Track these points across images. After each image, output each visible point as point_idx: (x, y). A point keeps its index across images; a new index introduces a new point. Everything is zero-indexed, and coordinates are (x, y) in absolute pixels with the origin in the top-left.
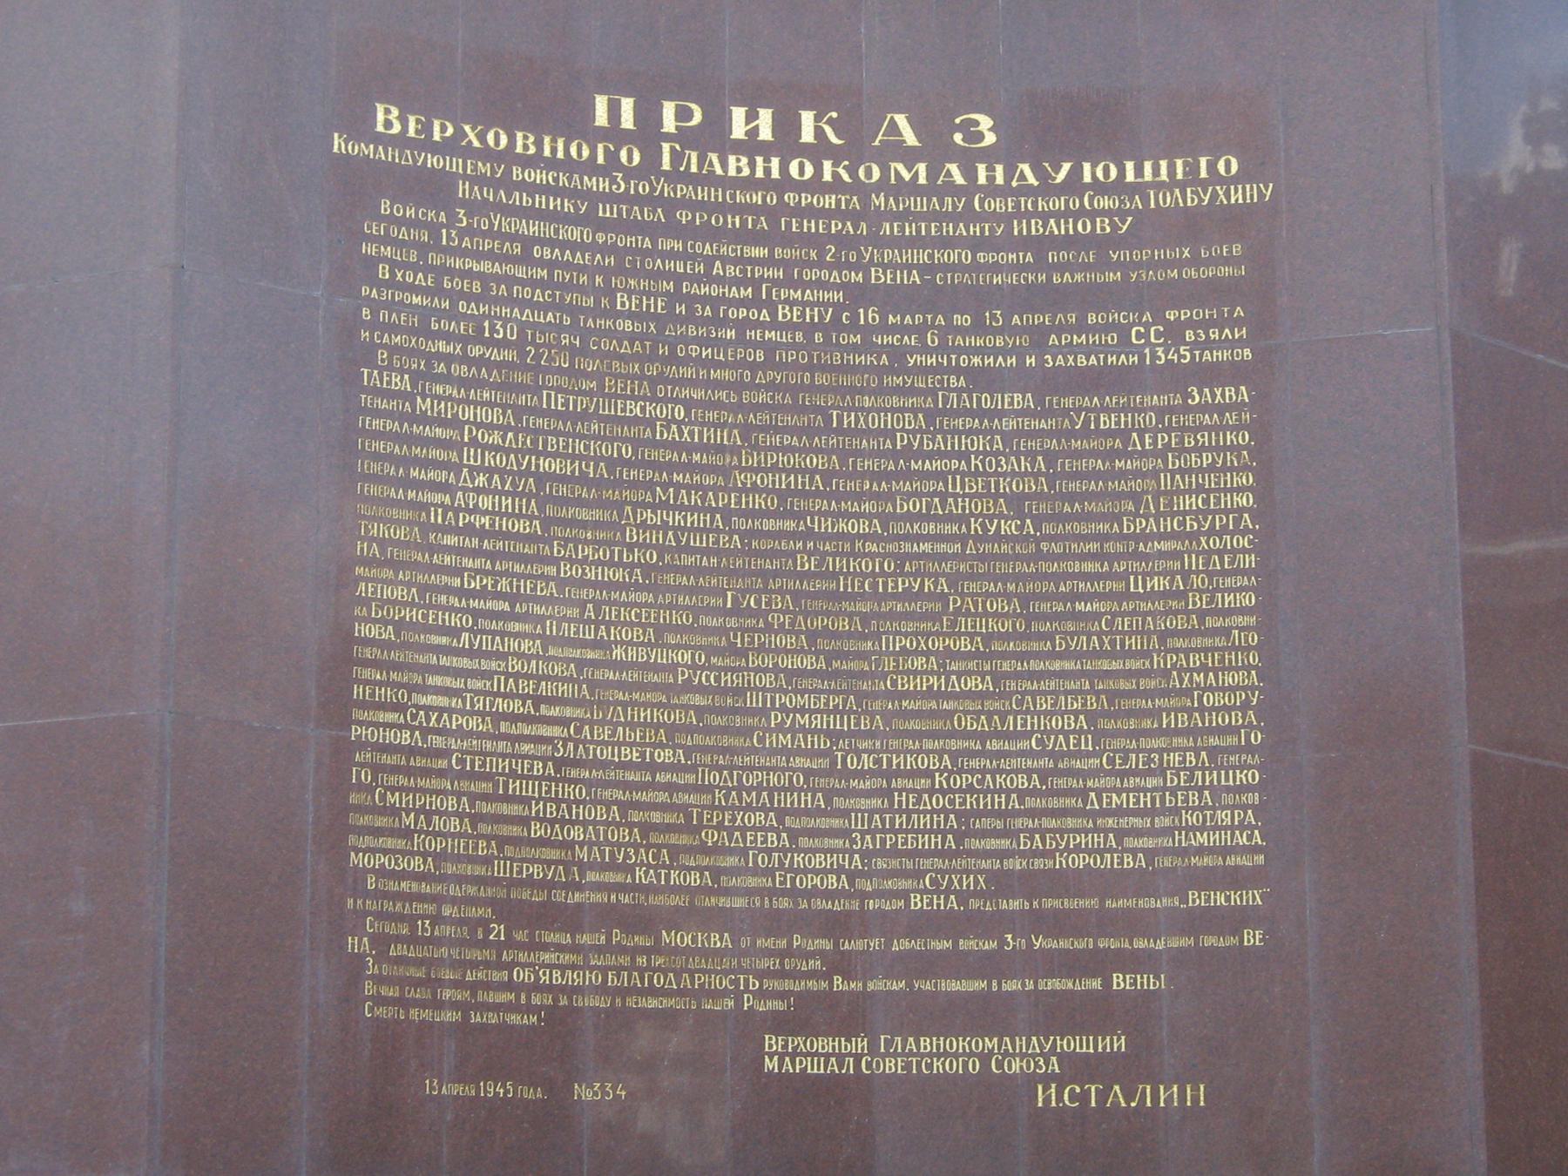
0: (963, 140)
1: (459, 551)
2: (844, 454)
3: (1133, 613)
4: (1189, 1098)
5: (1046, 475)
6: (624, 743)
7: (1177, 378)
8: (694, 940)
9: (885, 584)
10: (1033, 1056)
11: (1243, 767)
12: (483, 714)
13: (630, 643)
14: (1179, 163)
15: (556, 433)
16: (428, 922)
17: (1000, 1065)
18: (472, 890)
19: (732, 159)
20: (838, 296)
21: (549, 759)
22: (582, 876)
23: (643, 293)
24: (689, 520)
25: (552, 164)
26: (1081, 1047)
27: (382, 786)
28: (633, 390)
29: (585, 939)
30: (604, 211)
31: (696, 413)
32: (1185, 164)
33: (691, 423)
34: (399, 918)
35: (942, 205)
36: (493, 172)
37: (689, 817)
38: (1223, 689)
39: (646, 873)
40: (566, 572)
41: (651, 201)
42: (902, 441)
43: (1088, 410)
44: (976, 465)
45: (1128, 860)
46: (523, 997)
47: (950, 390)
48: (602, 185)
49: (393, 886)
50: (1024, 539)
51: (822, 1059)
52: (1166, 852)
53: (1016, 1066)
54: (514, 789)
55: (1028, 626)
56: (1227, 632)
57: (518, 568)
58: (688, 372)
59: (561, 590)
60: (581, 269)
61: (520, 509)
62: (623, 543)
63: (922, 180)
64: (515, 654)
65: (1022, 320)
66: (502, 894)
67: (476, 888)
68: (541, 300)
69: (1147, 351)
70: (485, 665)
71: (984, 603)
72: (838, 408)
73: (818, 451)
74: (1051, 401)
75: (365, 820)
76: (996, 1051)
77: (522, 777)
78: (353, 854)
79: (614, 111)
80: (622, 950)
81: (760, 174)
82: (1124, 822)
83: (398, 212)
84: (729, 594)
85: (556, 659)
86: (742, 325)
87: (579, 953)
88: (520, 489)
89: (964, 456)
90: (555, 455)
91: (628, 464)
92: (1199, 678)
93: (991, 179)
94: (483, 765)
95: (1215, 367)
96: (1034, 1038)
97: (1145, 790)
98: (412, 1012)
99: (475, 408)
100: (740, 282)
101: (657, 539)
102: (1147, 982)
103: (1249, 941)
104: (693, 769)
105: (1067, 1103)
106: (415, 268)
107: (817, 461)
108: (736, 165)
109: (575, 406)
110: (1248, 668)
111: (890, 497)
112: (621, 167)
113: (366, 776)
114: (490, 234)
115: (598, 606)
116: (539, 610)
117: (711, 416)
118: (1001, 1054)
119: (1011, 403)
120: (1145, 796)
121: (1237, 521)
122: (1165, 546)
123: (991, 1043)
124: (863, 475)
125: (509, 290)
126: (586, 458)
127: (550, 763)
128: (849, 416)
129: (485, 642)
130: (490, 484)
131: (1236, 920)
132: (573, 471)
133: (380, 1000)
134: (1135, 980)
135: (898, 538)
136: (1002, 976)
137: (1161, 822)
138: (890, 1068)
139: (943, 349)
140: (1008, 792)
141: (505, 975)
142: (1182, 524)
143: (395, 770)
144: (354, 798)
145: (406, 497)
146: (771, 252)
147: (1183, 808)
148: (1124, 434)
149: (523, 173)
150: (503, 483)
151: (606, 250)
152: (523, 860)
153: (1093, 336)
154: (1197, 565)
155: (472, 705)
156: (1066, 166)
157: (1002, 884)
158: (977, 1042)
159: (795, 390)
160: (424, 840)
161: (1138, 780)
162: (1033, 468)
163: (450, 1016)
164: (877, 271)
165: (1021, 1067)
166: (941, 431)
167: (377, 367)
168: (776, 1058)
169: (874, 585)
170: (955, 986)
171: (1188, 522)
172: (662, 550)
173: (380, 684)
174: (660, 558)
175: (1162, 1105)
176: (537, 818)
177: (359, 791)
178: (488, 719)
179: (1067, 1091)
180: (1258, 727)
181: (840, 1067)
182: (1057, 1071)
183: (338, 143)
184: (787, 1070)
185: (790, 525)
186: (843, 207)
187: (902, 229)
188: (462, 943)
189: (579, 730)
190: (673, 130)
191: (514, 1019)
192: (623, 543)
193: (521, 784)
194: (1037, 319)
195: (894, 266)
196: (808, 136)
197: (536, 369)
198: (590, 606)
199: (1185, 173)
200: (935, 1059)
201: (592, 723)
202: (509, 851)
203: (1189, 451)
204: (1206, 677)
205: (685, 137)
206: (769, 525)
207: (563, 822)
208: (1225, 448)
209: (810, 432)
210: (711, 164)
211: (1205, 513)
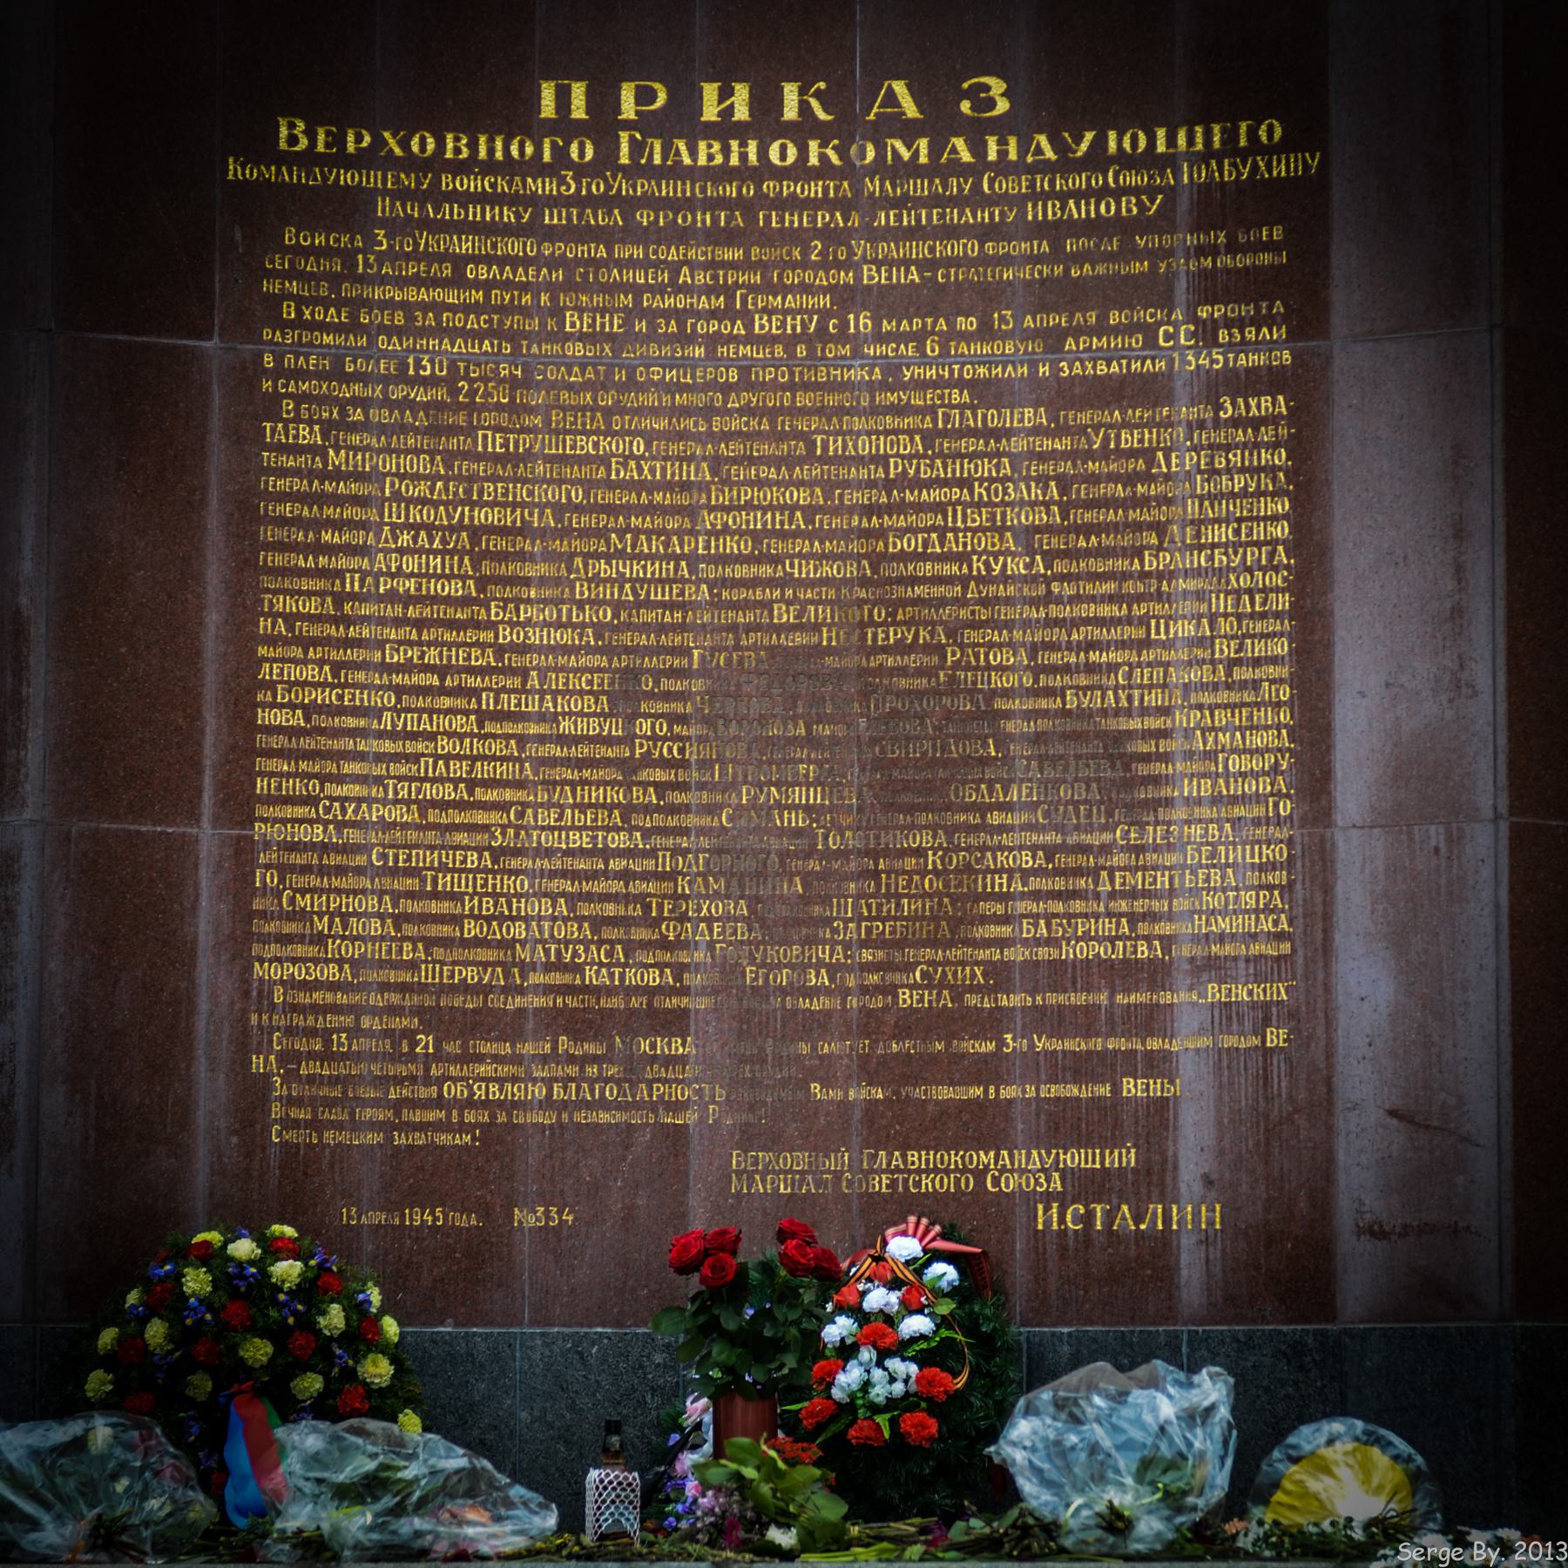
1: (382, 621)
2: (829, 486)
5: (1059, 504)
6: (573, 828)
9: (875, 636)
12: (408, 802)
13: (581, 714)
14: (1216, 128)
15: (495, 479)
17: (996, 1182)
18: (395, 998)
19: (702, 145)
20: (825, 301)
21: (485, 849)
22: (523, 977)
23: (594, 310)
24: (649, 570)
25: (490, 167)
28: (584, 424)
29: (528, 1049)
30: (551, 218)
32: (1223, 132)
33: (653, 458)
34: (311, 1033)
35: (945, 188)
36: (419, 183)
37: (647, 908)
38: (1251, 752)
39: (598, 972)
40: (505, 637)
41: (607, 202)
42: (896, 467)
44: (980, 495)
45: (1143, 951)
46: (455, 1113)
48: (547, 187)
49: (304, 999)
50: (1033, 579)
54: (445, 885)
55: (1036, 681)
56: (1256, 685)
57: (448, 637)
58: (650, 399)
60: (524, 287)
61: (452, 569)
62: (573, 601)
63: (923, 159)
64: (445, 733)
65: (1035, 322)
66: (429, 1002)
67: (399, 996)
69: (1176, 355)
71: (987, 655)
72: (825, 432)
73: (800, 484)
74: (1066, 417)
75: (271, 927)
77: (454, 870)
80: (571, 1059)
81: (734, 160)
82: (1140, 905)
84: (696, 652)
85: (495, 736)
86: (713, 341)
87: (520, 1064)
89: (965, 483)
90: (494, 504)
91: (578, 509)
93: (1003, 154)
94: (409, 859)
96: (1035, 1152)
98: (326, 1135)
100: (709, 291)
102: (1157, 1088)
104: (652, 853)
107: (801, 496)
108: (707, 153)
109: (516, 447)
112: (570, 164)
113: (272, 879)
114: (415, 256)
115: (543, 673)
116: (472, 682)
117: (675, 448)
124: (851, 510)
125: (438, 319)
126: (533, 505)
127: (486, 854)
128: (835, 442)
129: (410, 722)
130: (415, 542)
132: (514, 522)
133: (288, 1124)
134: (1148, 1085)
136: (999, 1080)
140: (1010, 872)
142: (1211, 558)
143: (306, 869)
144: (257, 904)
145: (316, 564)
146: (747, 253)
148: (1148, 454)
150: (431, 541)
151: (553, 263)
152: (454, 963)
155: (396, 793)
156: (1089, 136)
157: (1000, 977)
159: (773, 413)
162: (1044, 495)
163: (373, 1138)
164: (870, 270)
167: (282, 420)
170: (944, 1093)
172: (618, 606)
173: (289, 775)
174: (616, 615)
176: (471, 916)
180: (1288, 796)
182: (1060, 1189)
183: (234, 170)
185: (766, 571)
187: (899, 218)
189: (521, 815)
190: (632, 116)
191: (444, 1139)
192: (573, 601)
194: (1053, 320)
195: (889, 263)
196: (791, 113)
197: (471, 407)
199: (1223, 142)
202: (439, 953)
205: (648, 125)
206: (741, 571)
207: (501, 919)
208: (1259, 469)
209: (789, 461)
210: (678, 153)
211: (1236, 546)
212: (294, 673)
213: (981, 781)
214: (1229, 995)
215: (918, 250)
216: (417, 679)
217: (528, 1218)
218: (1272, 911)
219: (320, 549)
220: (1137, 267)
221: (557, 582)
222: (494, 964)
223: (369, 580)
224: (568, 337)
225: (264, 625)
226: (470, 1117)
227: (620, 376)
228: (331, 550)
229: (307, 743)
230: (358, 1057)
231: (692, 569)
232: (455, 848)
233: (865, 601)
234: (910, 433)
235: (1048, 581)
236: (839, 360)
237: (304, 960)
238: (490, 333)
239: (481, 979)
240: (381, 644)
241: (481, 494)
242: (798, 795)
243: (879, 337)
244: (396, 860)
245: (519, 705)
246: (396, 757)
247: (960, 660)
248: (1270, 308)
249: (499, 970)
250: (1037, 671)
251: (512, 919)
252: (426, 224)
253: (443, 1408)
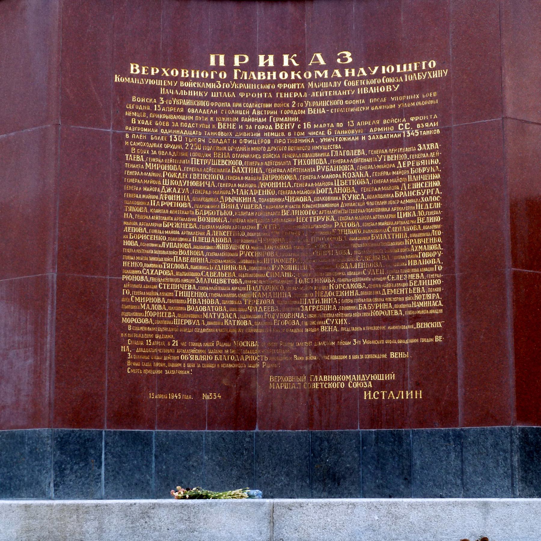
0: (341, 61)
1: (162, 215)
2: (298, 175)
3: (398, 226)
4: (416, 395)
5: (369, 178)
6: (221, 278)
7: (414, 141)
8: (245, 344)
9: (313, 219)
10: (363, 381)
11: (436, 278)
12: (170, 270)
13: (223, 243)
14: (415, 64)
15: (196, 172)
16: (150, 340)
17: (351, 385)
18: (166, 329)
19: (259, 73)
20: (296, 119)
21: (194, 284)
22: (206, 323)
23: (227, 122)
25: (195, 80)
26: (379, 378)
27: (134, 295)
29: (207, 345)
30: (214, 95)
31: (246, 163)
32: (418, 65)
33: (245, 166)
35: (333, 85)
36: (173, 84)
38: (429, 251)
39: (228, 321)
40: (200, 220)
41: (231, 90)
42: (319, 168)
43: (383, 154)
44: (344, 176)
45: (396, 313)
46: (184, 364)
47: (335, 150)
52: (410, 309)
53: (357, 385)
54: (181, 295)
55: (362, 232)
56: (430, 231)
57: (182, 220)
58: (244, 149)
59: (198, 226)
60: (205, 115)
61: (183, 199)
62: (220, 209)
63: (326, 76)
65: (361, 124)
67: (167, 328)
68: (191, 127)
69: (404, 132)
70: (171, 253)
71: (347, 224)
72: (296, 158)
73: (289, 174)
74: (370, 152)
75: (127, 307)
77: (184, 290)
78: (123, 318)
79: (217, 60)
80: (220, 348)
81: (269, 78)
82: (395, 299)
83: (139, 100)
84: (258, 225)
85: (196, 250)
86: (263, 131)
87: (204, 349)
88: (183, 192)
89: (340, 173)
90: (196, 180)
91: (222, 182)
92: (421, 247)
93: (350, 74)
94: (170, 287)
95: (426, 136)
96: (363, 375)
97: (402, 288)
98: (144, 371)
99: (167, 165)
100: (261, 116)
101: (232, 207)
102: (402, 355)
103: (437, 340)
104: (245, 285)
105: (374, 398)
106: (145, 119)
107: (289, 177)
108: (261, 76)
109: (203, 163)
110: (437, 243)
111: (314, 188)
112: (219, 79)
113: (128, 292)
116: (190, 233)
117: (252, 163)
119: (357, 153)
120: (402, 290)
121: (434, 191)
122: (410, 201)
123: (348, 377)
124: (305, 181)
126: (208, 181)
127: (194, 285)
128: (300, 161)
129: (171, 245)
130: (172, 191)
131: (432, 333)
132: (202, 185)
133: (133, 367)
134: (398, 354)
135: (317, 202)
136: (352, 354)
137: (408, 299)
139: (333, 135)
140: (355, 290)
141: (178, 358)
142: (415, 193)
143: (137, 290)
144: (123, 300)
145: (142, 197)
146: (273, 105)
147: (415, 294)
148: (396, 162)
149: (184, 84)
150: (177, 191)
151: (214, 108)
152: (184, 319)
153: (385, 128)
154: (421, 208)
155: (166, 267)
156: (376, 68)
157: (352, 322)
158: (344, 377)
159: (281, 153)
160: (149, 313)
161: (400, 284)
163: (159, 372)
164: (310, 110)
165: (359, 385)
166: (332, 164)
167: (131, 154)
169: (309, 220)
170: (335, 358)
171: (417, 192)
172: (234, 211)
173: (133, 261)
174: (233, 213)
175: (407, 398)
176: (189, 304)
177: (125, 297)
178: (172, 271)
179: (374, 393)
180: (441, 264)
182: (371, 387)
183: (117, 79)
185: (279, 200)
186: (298, 88)
187: (319, 94)
188: (162, 347)
189: (204, 274)
190: (238, 65)
191: (181, 372)
192: (220, 209)
193: (184, 292)
194: (366, 123)
195: (316, 107)
196: (286, 64)
197: (189, 151)
198: (209, 231)
199: (418, 68)
201: (209, 271)
202: (179, 315)
203: (418, 167)
204: (423, 247)
205: (242, 67)
206: (272, 200)
207: (199, 305)
208: (430, 166)
209: (286, 167)
210: (252, 76)
211: (423, 189)
212: (135, 230)
213: (346, 262)
214: (423, 326)
215: (325, 103)
216: (173, 232)
217: (206, 397)
218: (437, 300)
219: (142, 192)
220: (392, 106)
221: (217, 203)
222: (197, 319)
223: (158, 202)
224: (219, 130)
225: (126, 215)
226: (189, 366)
227: (234, 142)
228: (147, 193)
229: (138, 251)
230: (154, 347)
231: (257, 200)
232: (185, 284)
233: (310, 209)
234: (323, 158)
235: (365, 201)
236: (301, 137)
237: (138, 317)
238: (195, 129)
239: (192, 323)
240: (161, 222)
241: (192, 177)
242: (290, 268)
243: (313, 129)
244: (166, 287)
245: (204, 240)
246: (166, 256)
247: (339, 226)
248: (433, 117)
249: (198, 320)
250: (362, 229)
251: (202, 305)
252: (175, 96)
253: (181, 455)
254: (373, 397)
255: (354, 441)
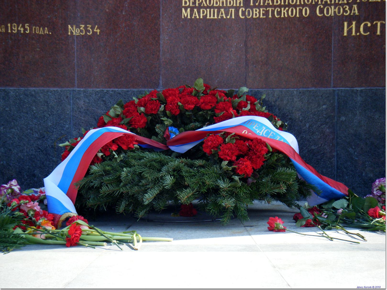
10: (342, 5)
51: (216, 10)
53: (332, 11)
76: (320, 3)
105: (362, 32)
118: (323, 5)
138: (256, 14)
165: (335, 12)
168: (189, 10)
179: (362, 26)
181: (227, 15)
182: (357, 13)
184: (195, 17)
200: (283, 9)
253: (31, 129)
254: (360, 32)
255: (324, 107)
